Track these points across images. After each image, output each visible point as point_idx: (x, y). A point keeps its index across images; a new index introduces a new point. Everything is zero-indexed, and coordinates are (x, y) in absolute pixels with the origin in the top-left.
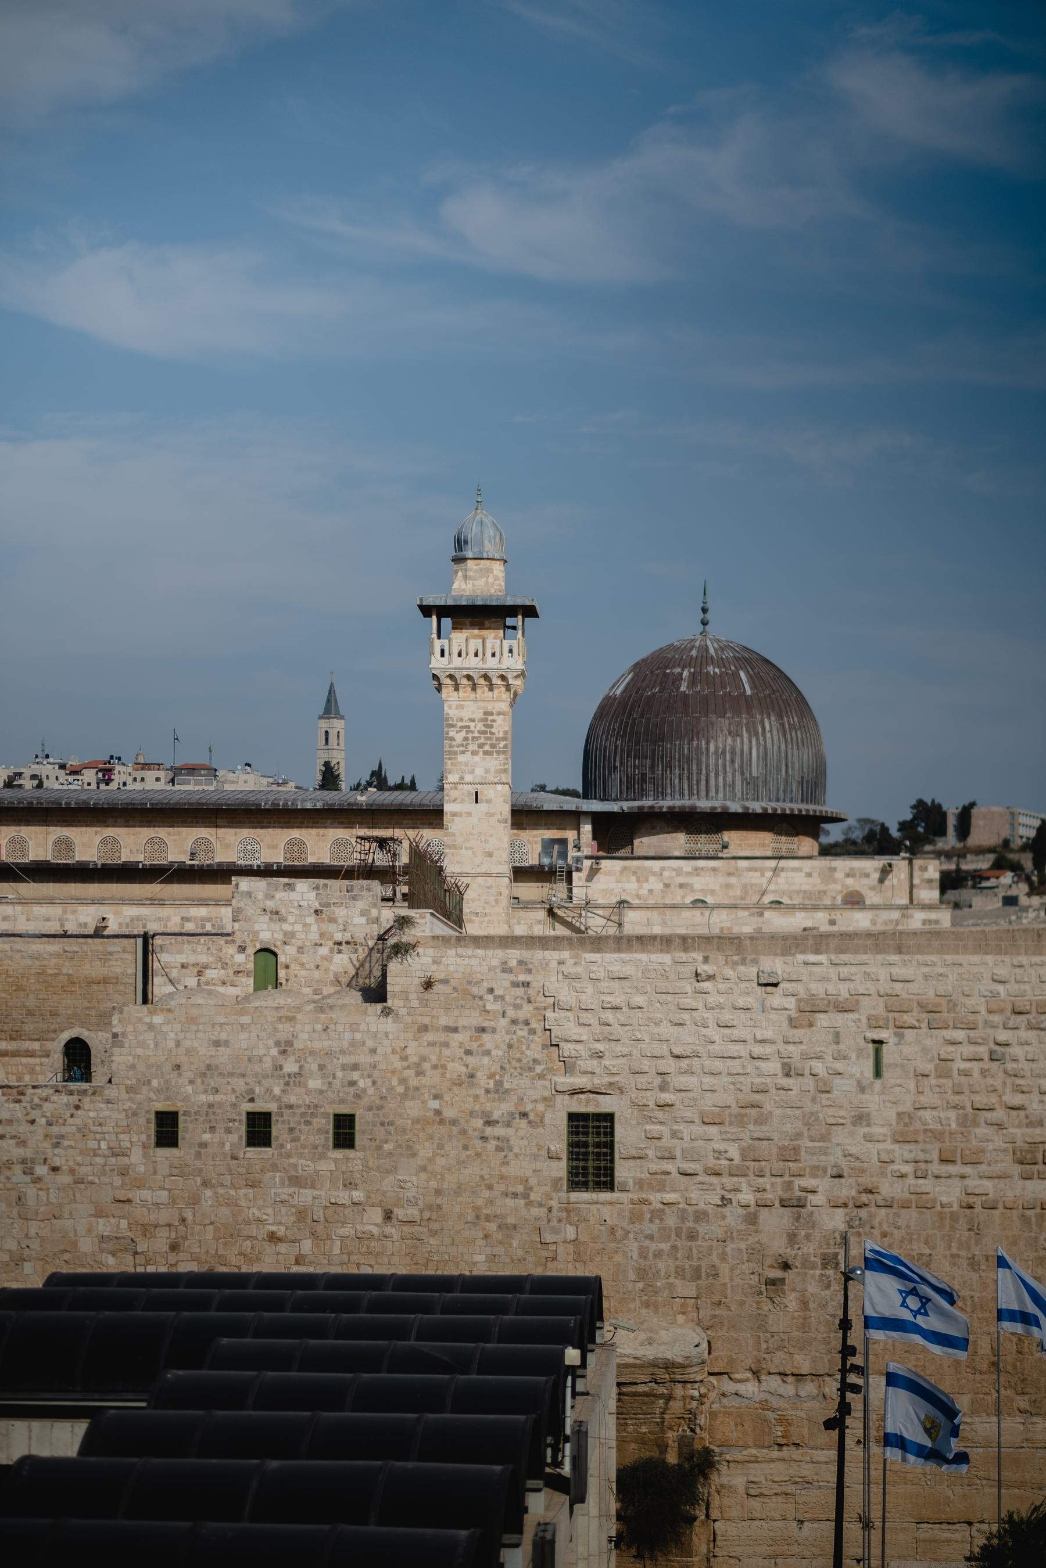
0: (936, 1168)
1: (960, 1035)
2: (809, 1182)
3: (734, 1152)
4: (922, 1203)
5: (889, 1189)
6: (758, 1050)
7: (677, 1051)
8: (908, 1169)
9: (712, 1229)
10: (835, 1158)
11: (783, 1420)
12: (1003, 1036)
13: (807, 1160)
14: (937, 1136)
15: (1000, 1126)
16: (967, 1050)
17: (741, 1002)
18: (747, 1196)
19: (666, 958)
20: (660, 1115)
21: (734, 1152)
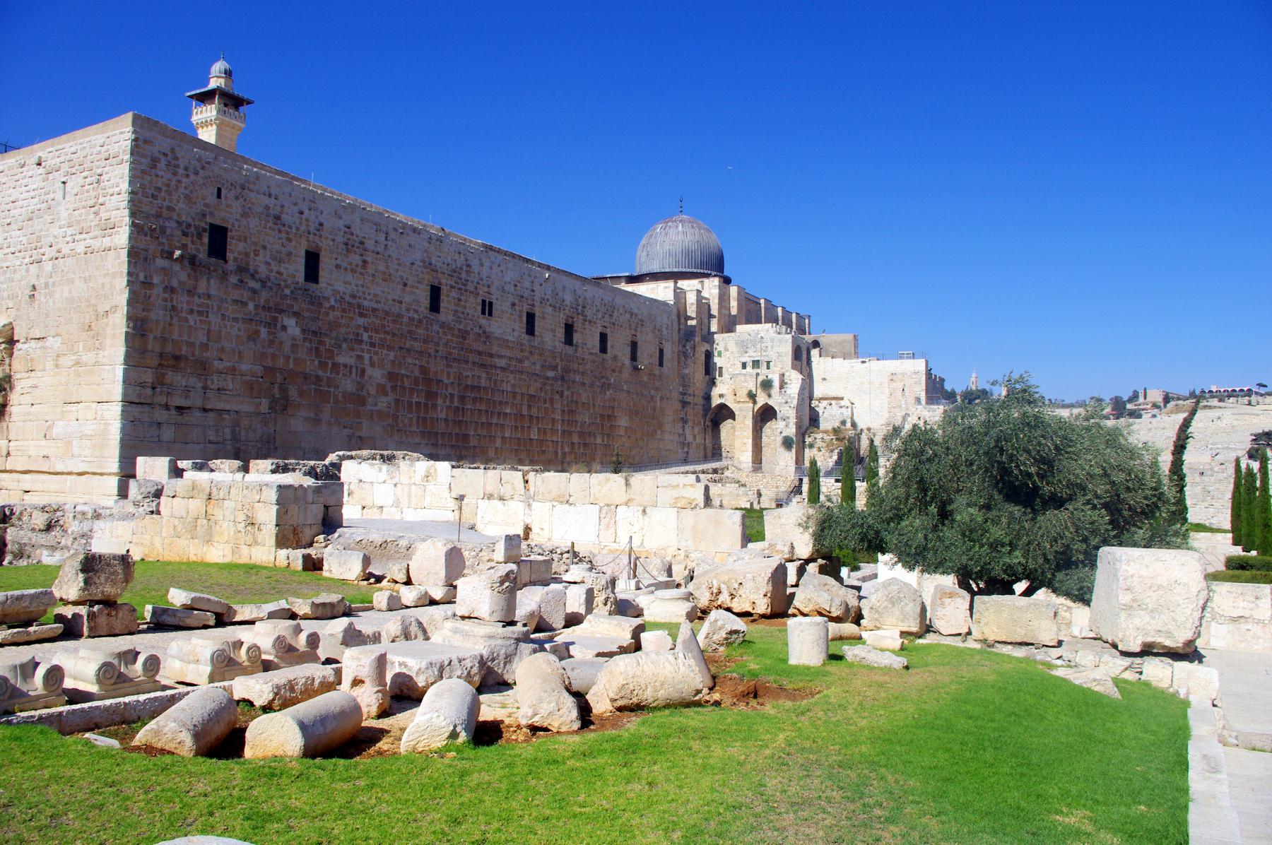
0: (78, 237)
1: (86, 174)
2: (42, 251)
3: (24, 239)
4: (73, 254)
5: (66, 250)
6: (32, 194)
7: (12, 199)
8: (68, 239)
9: (18, 276)
10: (51, 239)
11: (32, 360)
12: (99, 171)
13: (44, 241)
14: (78, 222)
15: (96, 213)
16: (89, 180)
17: (30, 174)
18: (27, 260)
19: (13, 160)
20: (7, 228)
21: (24, 239)
